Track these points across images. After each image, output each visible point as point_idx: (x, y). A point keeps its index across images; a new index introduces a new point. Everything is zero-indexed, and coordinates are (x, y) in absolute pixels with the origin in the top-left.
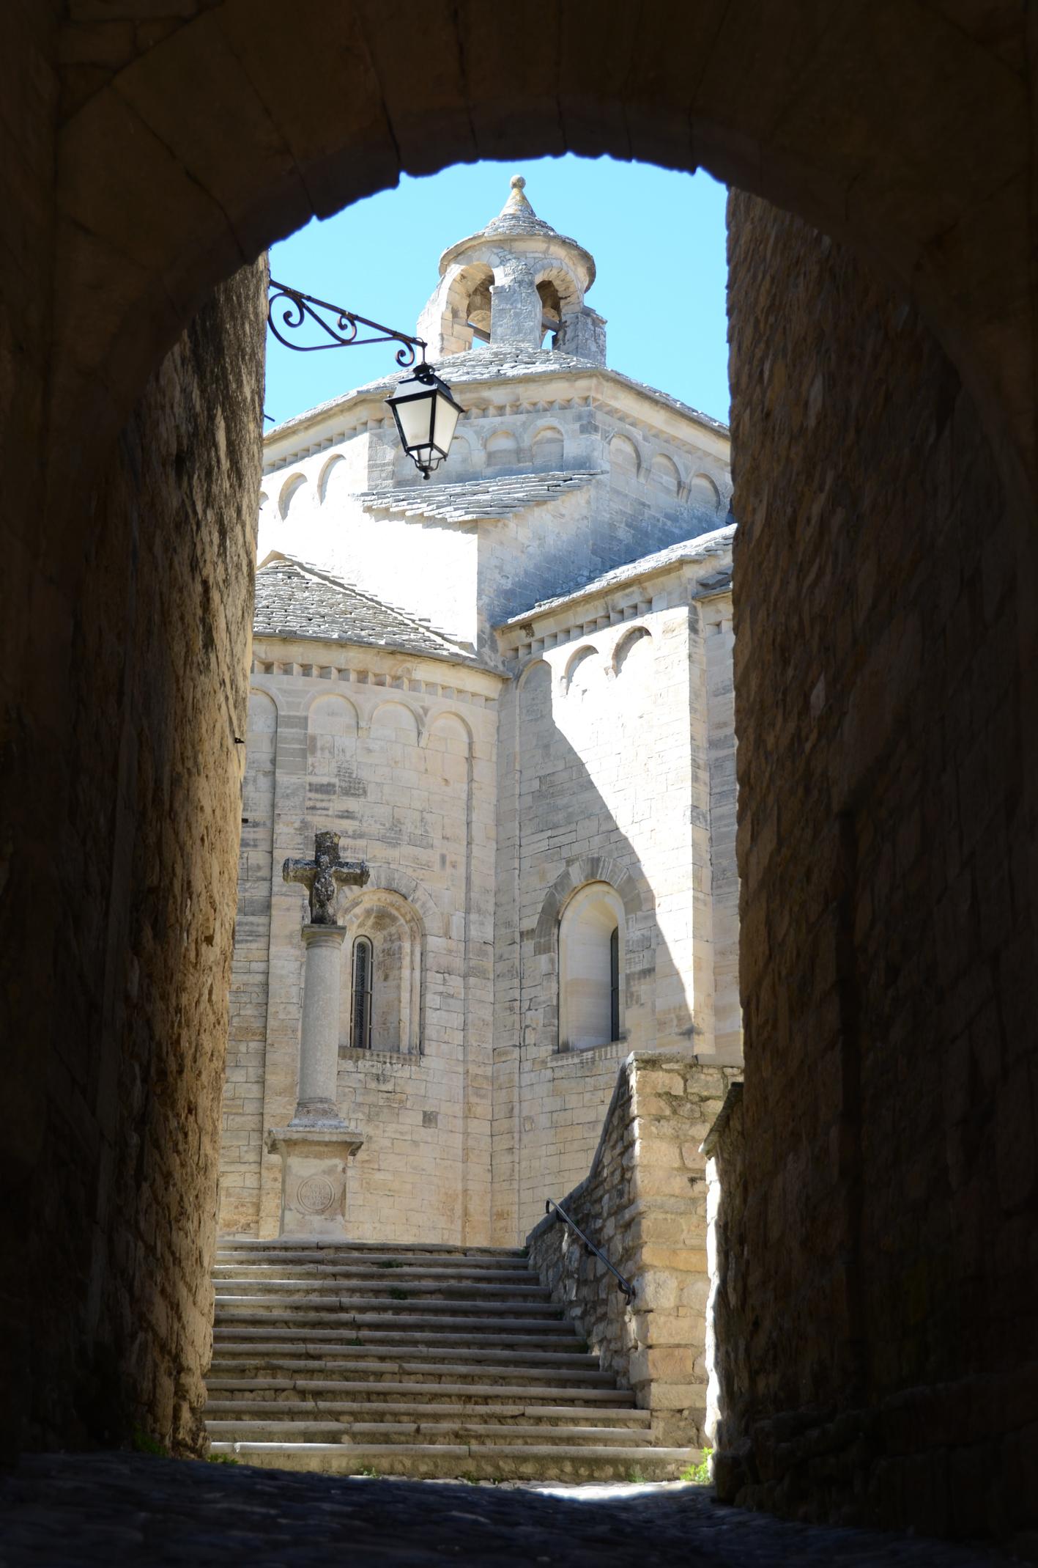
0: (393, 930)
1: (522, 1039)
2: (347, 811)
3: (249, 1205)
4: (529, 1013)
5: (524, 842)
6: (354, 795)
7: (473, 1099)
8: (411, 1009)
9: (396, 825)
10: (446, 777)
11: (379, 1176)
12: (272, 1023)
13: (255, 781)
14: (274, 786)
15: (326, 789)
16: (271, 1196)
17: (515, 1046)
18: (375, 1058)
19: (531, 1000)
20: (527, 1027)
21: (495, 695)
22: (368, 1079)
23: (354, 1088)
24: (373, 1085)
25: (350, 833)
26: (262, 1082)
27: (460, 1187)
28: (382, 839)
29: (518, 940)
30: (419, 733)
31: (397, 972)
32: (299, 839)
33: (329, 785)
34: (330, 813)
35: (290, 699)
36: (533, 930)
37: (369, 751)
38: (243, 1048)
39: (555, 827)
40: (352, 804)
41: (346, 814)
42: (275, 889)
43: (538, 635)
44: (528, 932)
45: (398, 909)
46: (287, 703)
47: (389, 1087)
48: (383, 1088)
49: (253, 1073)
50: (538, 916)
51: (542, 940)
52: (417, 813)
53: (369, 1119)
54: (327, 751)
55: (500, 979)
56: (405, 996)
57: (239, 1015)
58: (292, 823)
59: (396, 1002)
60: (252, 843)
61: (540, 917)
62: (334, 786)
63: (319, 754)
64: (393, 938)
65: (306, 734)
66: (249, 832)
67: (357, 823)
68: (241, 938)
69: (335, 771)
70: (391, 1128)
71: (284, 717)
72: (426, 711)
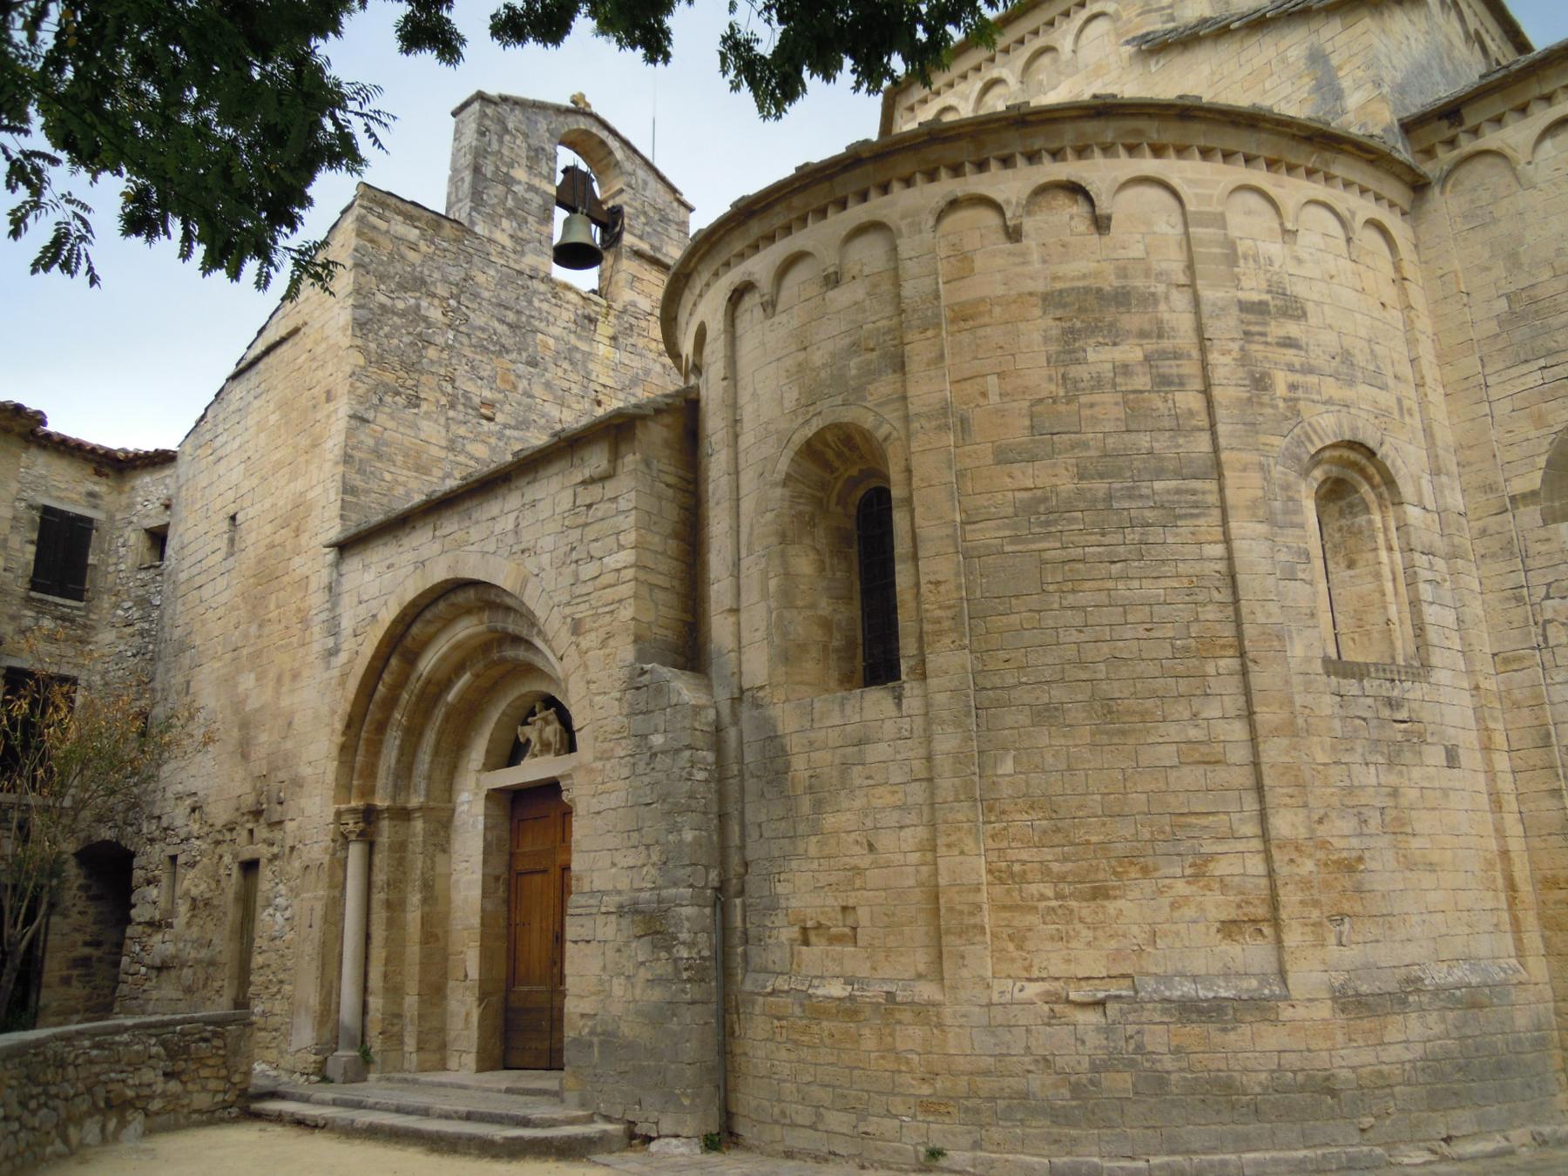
0: (1354, 498)
1: (1541, 639)
2: (1289, 338)
3: (1257, 902)
4: (1549, 602)
5: (1490, 380)
6: (1292, 317)
7: (1492, 725)
8: (1398, 604)
9: (1346, 356)
10: (1383, 300)
11: (1415, 843)
12: (1250, 631)
13: (1167, 298)
14: (1196, 302)
15: (1259, 308)
16: (1290, 887)
17: (1533, 648)
18: (1381, 675)
19: (1549, 585)
20: (1547, 622)
21: (1407, 207)
22: (1379, 704)
23: (1364, 719)
24: (1386, 713)
25: (1298, 367)
26: (1249, 715)
27: (1493, 845)
28: (1336, 376)
29: (1509, 506)
30: (1349, 240)
31: (1370, 556)
32: (1241, 373)
33: (1261, 303)
34: (1269, 339)
35: (1199, 191)
36: (1534, 493)
37: (1299, 261)
38: (1210, 668)
39: (1550, 353)
40: (1293, 329)
41: (1288, 341)
42: (1222, 442)
43: (1470, 122)
44: (1524, 496)
45: (1362, 471)
46: (1197, 195)
47: (1403, 715)
48: (1399, 716)
49: (1234, 703)
50: (1541, 472)
51: (1557, 504)
52: (1365, 344)
53: (1391, 764)
54: (1251, 262)
55: (1488, 561)
56: (1389, 586)
57: (1197, 620)
58: (1229, 352)
59: (1377, 595)
60: (1177, 381)
61: (1545, 473)
62: (1266, 303)
63: (1242, 262)
64: (1355, 510)
65: (1226, 235)
66: (1171, 366)
67: (1303, 353)
68: (1183, 511)
69: (1264, 285)
70: (1416, 773)
71: (1195, 213)
72: (1353, 214)
